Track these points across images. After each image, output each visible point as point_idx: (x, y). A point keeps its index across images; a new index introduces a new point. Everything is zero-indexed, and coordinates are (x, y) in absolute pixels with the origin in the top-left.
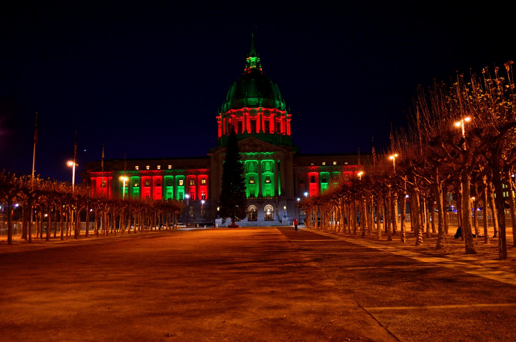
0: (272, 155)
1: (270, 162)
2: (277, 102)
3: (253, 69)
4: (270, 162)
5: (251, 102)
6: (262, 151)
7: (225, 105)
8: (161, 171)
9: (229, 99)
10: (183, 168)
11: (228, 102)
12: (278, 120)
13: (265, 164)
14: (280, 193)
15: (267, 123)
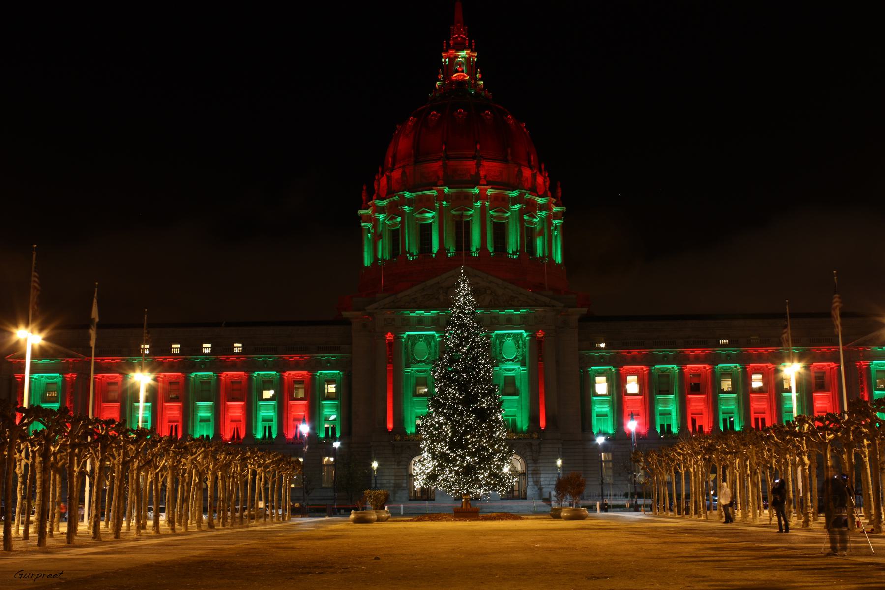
0: (521, 316)
1: (517, 338)
2: (527, 173)
3: (461, 83)
4: (515, 335)
6: (495, 307)
7: (384, 181)
8: (213, 358)
9: (394, 164)
10: (274, 351)
11: (392, 170)
12: (531, 222)
13: (502, 343)
14: (543, 424)
15: (500, 232)
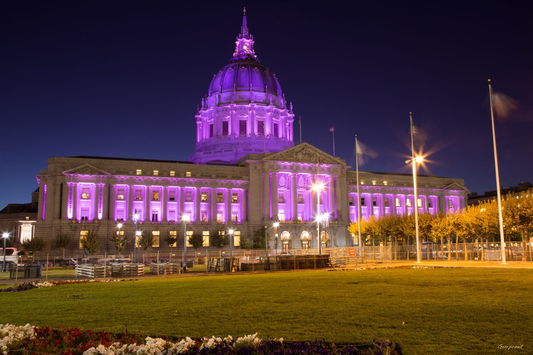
0: (328, 168)
5: (256, 97)
9: (221, 89)
